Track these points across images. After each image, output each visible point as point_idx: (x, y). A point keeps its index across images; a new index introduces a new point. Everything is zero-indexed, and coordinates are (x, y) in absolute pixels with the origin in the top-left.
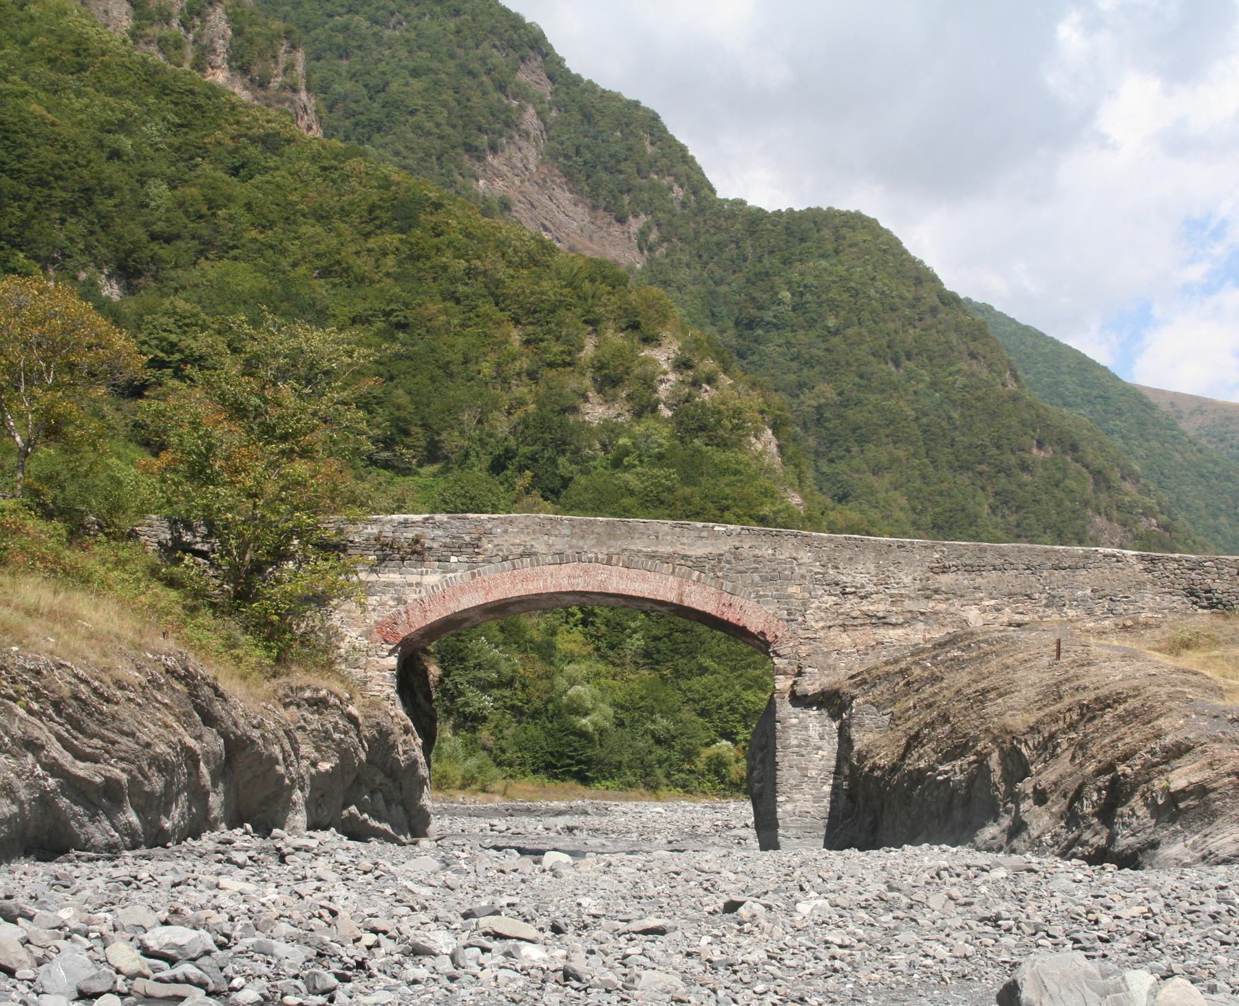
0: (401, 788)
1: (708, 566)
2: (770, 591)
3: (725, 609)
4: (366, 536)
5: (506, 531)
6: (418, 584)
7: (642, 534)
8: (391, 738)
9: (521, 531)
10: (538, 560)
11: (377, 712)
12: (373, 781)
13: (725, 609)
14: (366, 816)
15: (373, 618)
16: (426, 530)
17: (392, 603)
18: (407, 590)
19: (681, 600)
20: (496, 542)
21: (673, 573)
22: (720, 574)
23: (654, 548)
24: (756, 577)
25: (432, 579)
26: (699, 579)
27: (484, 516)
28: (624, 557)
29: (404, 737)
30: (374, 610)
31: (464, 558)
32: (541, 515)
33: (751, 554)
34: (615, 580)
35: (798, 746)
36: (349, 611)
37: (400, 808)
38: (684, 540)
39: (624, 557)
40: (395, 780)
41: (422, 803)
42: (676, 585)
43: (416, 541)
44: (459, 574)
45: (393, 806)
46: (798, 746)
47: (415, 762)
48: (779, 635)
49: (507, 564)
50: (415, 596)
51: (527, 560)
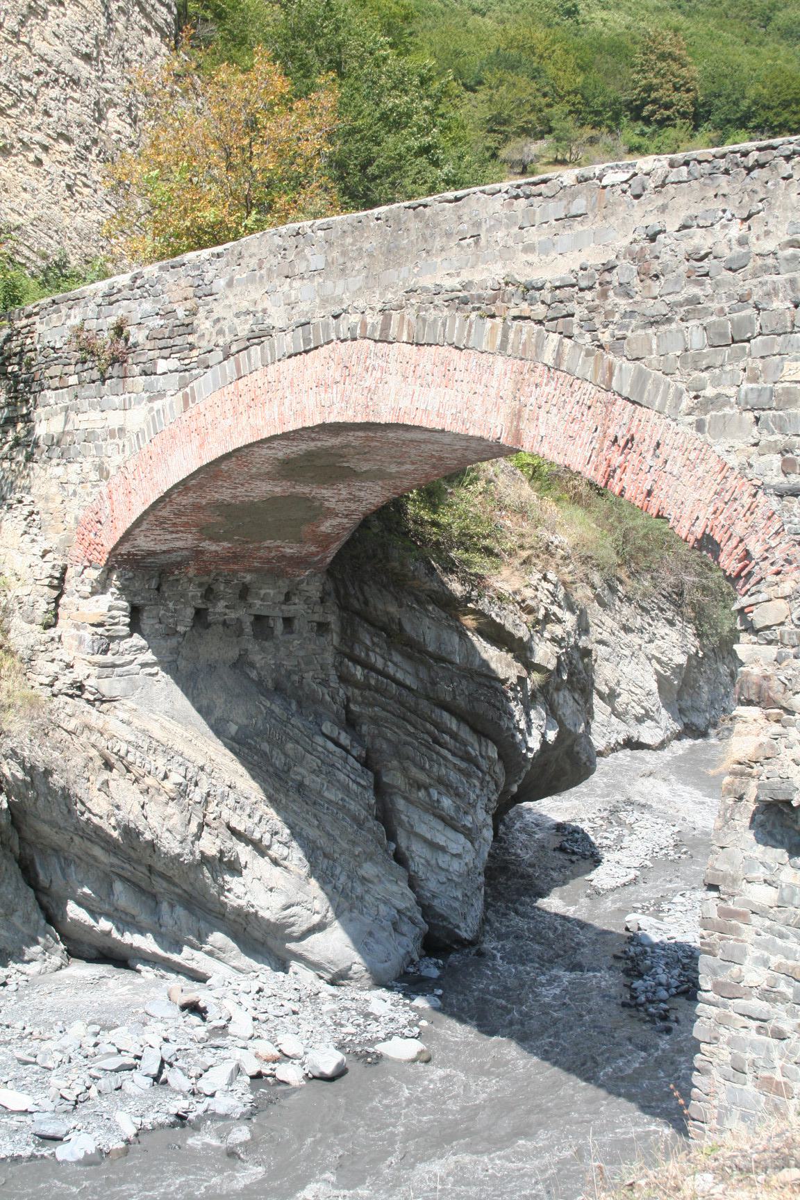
0: (162, 876)
1: (580, 312)
2: (732, 380)
3: (617, 460)
4: (67, 333)
5: (230, 284)
6: (121, 430)
7: (448, 235)
8: (57, 780)
9: (251, 280)
10: (272, 347)
11: (15, 728)
12: (95, 859)
13: (617, 460)
14: (105, 925)
15: (75, 510)
16: (133, 305)
17: (94, 476)
18: (109, 447)
19: (517, 436)
20: (215, 316)
21: (503, 346)
22: (605, 337)
23: (466, 276)
24: (697, 339)
25: (137, 418)
26: (559, 355)
27: (205, 253)
28: (410, 314)
29: (106, 775)
30: (75, 493)
31: (173, 363)
32: (283, 229)
33: (685, 246)
34: (394, 381)
35: (769, 995)
36: (47, 499)
37: (180, 911)
38: (532, 236)
39: (410, 314)
40: (129, 860)
41: (231, 900)
42: (508, 385)
43: (119, 330)
44: (167, 400)
45: (165, 906)
46: (769, 995)
47: (130, 833)
48: (757, 550)
49: (229, 365)
50: (117, 459)
51: (255, 351)
